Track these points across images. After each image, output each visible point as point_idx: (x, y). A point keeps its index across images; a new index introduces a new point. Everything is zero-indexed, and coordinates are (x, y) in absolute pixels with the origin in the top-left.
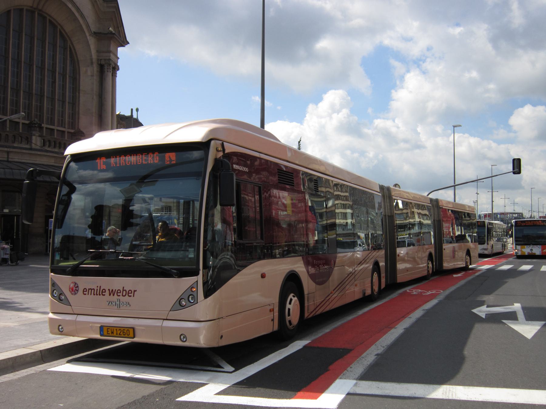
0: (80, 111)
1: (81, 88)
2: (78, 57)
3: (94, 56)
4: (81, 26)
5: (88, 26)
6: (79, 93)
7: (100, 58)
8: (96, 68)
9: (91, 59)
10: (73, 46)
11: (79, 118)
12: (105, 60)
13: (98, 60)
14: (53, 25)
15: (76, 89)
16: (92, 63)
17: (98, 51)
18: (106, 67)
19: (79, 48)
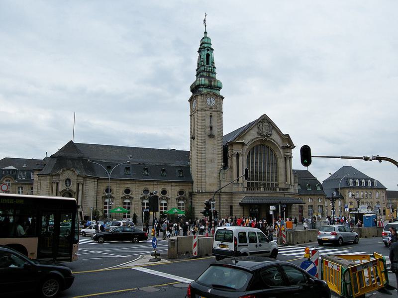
3: (282, 155)
5: (279, 146)
8: (283, 159)
14: (268, 147)
15: (277, 167)
19: (277, 153)
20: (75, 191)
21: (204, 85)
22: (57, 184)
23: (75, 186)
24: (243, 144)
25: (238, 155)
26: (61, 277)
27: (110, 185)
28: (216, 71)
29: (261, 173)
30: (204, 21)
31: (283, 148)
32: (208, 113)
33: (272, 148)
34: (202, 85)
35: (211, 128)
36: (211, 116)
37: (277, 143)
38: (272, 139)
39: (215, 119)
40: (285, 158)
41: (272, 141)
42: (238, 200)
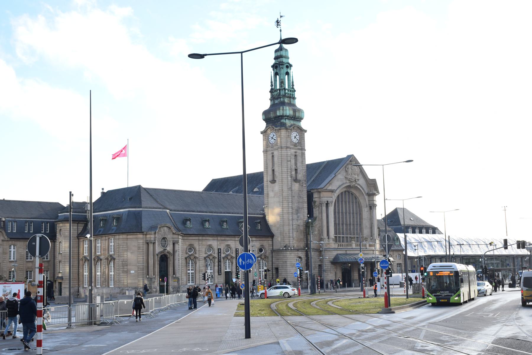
0: (364, 228)
1: (363, 218)
2: (362, 204)
3: (368, 203)
4: (363, 193)
6: (363, 220)
7: (370, 203)
8: (368, 208)
9: (367, 205)
10: (359, 201)
11: (363, 230)
12: (372, 204)
13: (369, 204)
14: (352, 194)
15: (361, 218)
16: (367, 207)
17: (369, 201)
18: (372, 207)
20: (172, 252)
21: (288, 116)
22: (154, 243)
23: (172, 246)
24: (332, 191)
25: (327, 204)
26: (106, 346)
27: (192, 242)
28: (296, 95)
29: (346, 224)
32: (293, 151)
34: (286, 116)
35: (296, 170)
36: (296, 155)
37: (361, 187)
38: (359, 185)
39: (299, 158)
41: (359, 187)
42: (329, 256)
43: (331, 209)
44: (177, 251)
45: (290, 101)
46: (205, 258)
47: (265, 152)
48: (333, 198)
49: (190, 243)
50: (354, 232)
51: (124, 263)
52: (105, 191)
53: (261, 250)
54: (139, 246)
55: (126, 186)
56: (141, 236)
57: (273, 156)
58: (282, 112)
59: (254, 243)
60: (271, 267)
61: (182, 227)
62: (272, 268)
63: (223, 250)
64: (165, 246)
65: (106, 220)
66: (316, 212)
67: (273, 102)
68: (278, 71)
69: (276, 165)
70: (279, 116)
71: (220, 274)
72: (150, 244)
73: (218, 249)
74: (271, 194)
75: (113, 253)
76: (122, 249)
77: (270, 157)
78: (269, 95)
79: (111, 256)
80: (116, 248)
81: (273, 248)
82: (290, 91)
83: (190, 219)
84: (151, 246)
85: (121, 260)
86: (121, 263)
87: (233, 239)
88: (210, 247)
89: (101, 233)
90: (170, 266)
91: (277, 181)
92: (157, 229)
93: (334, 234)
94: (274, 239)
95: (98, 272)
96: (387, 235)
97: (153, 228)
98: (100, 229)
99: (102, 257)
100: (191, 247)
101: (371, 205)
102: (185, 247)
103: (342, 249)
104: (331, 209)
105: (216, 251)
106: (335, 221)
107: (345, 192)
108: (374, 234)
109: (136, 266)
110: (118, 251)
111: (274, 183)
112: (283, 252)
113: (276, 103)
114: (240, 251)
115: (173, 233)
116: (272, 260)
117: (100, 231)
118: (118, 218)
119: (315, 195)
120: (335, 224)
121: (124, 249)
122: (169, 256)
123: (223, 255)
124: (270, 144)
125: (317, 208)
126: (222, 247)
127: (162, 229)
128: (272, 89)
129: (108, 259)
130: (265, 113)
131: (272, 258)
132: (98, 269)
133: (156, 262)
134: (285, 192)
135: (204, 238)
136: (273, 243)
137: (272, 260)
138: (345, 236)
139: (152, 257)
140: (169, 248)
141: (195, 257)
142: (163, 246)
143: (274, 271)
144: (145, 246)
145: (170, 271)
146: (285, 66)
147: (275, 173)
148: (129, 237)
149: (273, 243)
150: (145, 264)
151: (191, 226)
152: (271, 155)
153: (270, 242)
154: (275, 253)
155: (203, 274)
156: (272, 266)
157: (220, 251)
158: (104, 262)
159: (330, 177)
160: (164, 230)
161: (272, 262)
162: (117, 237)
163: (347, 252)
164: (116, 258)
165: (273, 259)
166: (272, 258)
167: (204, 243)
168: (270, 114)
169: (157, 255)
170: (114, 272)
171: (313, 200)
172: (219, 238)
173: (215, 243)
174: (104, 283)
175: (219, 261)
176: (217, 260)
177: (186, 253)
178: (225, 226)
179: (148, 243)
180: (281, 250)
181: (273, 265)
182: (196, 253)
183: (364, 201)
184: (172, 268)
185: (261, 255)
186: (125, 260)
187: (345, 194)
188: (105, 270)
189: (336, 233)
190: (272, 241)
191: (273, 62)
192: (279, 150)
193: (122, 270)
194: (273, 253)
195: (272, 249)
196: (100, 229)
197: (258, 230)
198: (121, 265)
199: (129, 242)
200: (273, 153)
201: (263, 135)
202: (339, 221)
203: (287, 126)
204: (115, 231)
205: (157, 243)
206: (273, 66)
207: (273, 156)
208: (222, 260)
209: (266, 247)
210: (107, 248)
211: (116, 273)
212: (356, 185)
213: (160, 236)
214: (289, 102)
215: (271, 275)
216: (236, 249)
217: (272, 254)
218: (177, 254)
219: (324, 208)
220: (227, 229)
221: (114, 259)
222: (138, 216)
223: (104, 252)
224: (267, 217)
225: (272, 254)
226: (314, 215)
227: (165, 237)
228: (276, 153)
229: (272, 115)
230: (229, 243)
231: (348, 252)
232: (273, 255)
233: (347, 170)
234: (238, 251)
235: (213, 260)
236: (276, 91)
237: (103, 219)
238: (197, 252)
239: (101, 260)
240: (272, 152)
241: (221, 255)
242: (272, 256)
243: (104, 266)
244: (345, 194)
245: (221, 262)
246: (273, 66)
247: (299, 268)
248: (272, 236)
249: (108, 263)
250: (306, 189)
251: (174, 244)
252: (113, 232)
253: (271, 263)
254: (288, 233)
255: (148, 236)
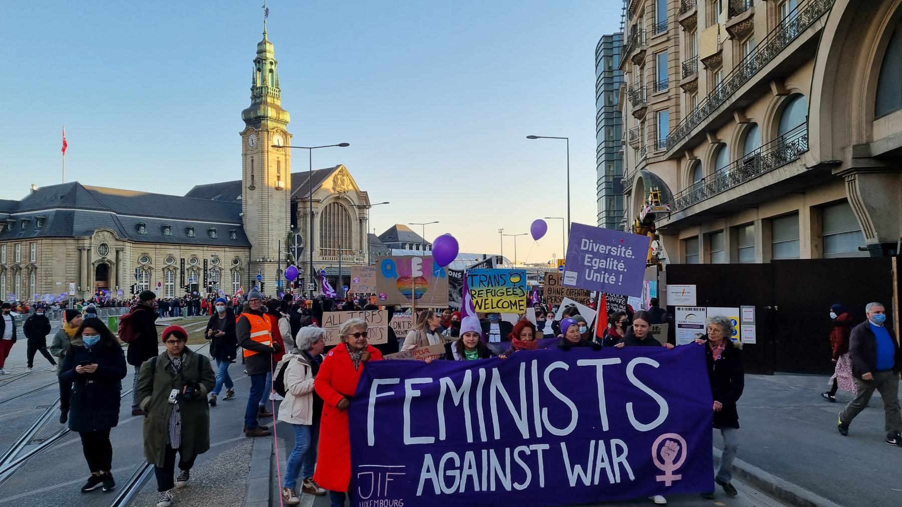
3: (358, 217)
8: (358, 221)
15: (350, 232)
20: (114, 261)
30: (267, 14)
31: (359, 207)
33: (347, 207)
40: (361, 220)
41: (348, 198)
43: (317, 220)
44: (122, 260)
45: (274, 102)
46: (163, 269)
47: (245, 155)
48: (319, 209)
49: (144, 252)
50: (346, 246)
51: (47, 272)
52: (35, 188)
53: (236, 262)
54: (68, 253)
55: (61, 183)
56: (72, 241)
57: (253, 160)
58: (263, 112)
59: (227, 254)
60: (248, 280)
61: (135, 233)
62: (249, 281)
63: (188, 261)
64: (104, 254)
65: (29, 221)
66: (300, 223)
67: (254, 101)
68: (260, 67)
69: (255, 171)
70: (260, 117)
71: (183, 287)
72: (83, 251)
73: (181, 259)
74: (250, 202)
75: (35, 261)
76: (45, 256)
77: (249, 161)
78: (250, 94)
79: (32, 264)
80: (38, 254)
81: (250, 260)
82: (274, 91)
83: (145, 225)
84: (85, 253)
85: (43, 270)
86: (43, 272)
87: (201, 248)
88: (170, 258)
89: (21, 237)
90: (112, 277)
91: (256, 187)
92: (93, 234)
93: (319, 246)
94: (251, 250)
95: (17, 283)
96: (298, 236)
97: (89, 233)
98: (21, 232)
99: (21, 266)
100: (145, 258)
101: (361, 218)
102: (137, 256)
103: (327, 262)
104: (317, 220)
105: (179, 262)
106: (321, 233)
107: (334, 203)
108: (363, 248)
109: (64, 276)
110: (40, 259)
111: (254, 189)
112: (260, 265)
113: (257, 102)
114: (209, 262)
115: (117, 240)
116: (249, 272)
117: (21, 234)
118: (43, 220)
119: (300, 205)
120: (321, 237)
121: (47, 256)
122: (110, 266)
123: (187, 266)
124: (250, 147)
125: (302, 219)
126: (187, 257)
127: (100, 234)
128: (253, 87)
129: (28, 268)
130: (245, 112)
131: (249, 270)
132: (18, 280)
133: (92, 273)
134: (264, 199)
135: (163, 247)
136: (250, 254)
137: (249, 272)
138: (328, 249)
139: (86, 266)
140: (111, 256)
141: (150, 268)
142: (102, 254)
143: (250, 284)
144: (76, 253)
145: (112, 283)
146: (268, 62)
147: (255, 179)
148: (54, 242)
149: (250, 254)
150: (76, 275)
151: (146, 232)
152: (251, 159)
153: (247, 254)
154: (253, 265)
155: (131, 287)
156: (249, 279)
157: (184, 262)
158: (24, 271)
159: (316, 186)
160: (103, 235)
161: (249, 274)
162: (40, 242)
163: (332, 265)
164: (38, 267)
165: (250, 271)
166: (249, 270)
167: (163, 252)
168: (250, 114)
169: (93, 264)
170: (36, 283)
171: (298, 210)
172: (182, 247)
173: (177, 252)
174: (24, 297)
175: (182, 273)
176: (179, 271)
177: (138, 263)
178: (214, 235)
179: (80, 250)
180: (257, 262)
181: (250, 277)
182: (151, 263)
183: (354, 214)
184: (115, 280)
185: (236, 267)
186: (49, 270)
187: (334, 206)
188: (25, 281)
189: (321, 246)
190: (250, 252)
191: (255, 56)
192: (259, 154)
193: (44, 281)
194: (250, 265)
195: (249, 261)
196: (21, 232)
197: (233, 239)
198: (44, 275)
199: (55, 248)
200: (253, 157)
201: (243, 137)
202: (326, 234)
203: (269, 128)
204: (38, 235)
205: (93, 250)
206: (255, 61)
207: (253, 160)
208: (186, 271)
209: (242, 258)
210: (28, 255)
211: (37, 285)
212: (345, 197)
213: (98, 242)
214: (272, 102)
215: (248, 288)
216: (205, 260)
217: (249, 266)
218: (121, 264)
219: (309, 219)
220: (194, 237)
221: (36, 268)
222: (69, 217)
223: (25, 259)
224: (244, 226)
225: (249, 266)
226: (298, 226)
227: (104, 243)
228: (255, 157)
229: (252, 115)
230: (195, 253)
231: (333, 266)
232: (250, 267)
233: (336, 181)
234: (207, 262)
235: (174, 271)
236: (257, 89)
237: (24, 221)
238: (153, 262)
239: (21, 269)
240: (252, 155)
241: (184, 266)
242: (249, 268)
243: (24, 276)
244: (334, 206)
245: (184, 273)
246: (255, 61)
247: (260, 281)
248: (250, 247)
249: (13, 273)
250: (290, 198)
251: (117, 252)
252: (35, 236)
253: (248, 275)
254: (267, 244)
255: (81, 242)
